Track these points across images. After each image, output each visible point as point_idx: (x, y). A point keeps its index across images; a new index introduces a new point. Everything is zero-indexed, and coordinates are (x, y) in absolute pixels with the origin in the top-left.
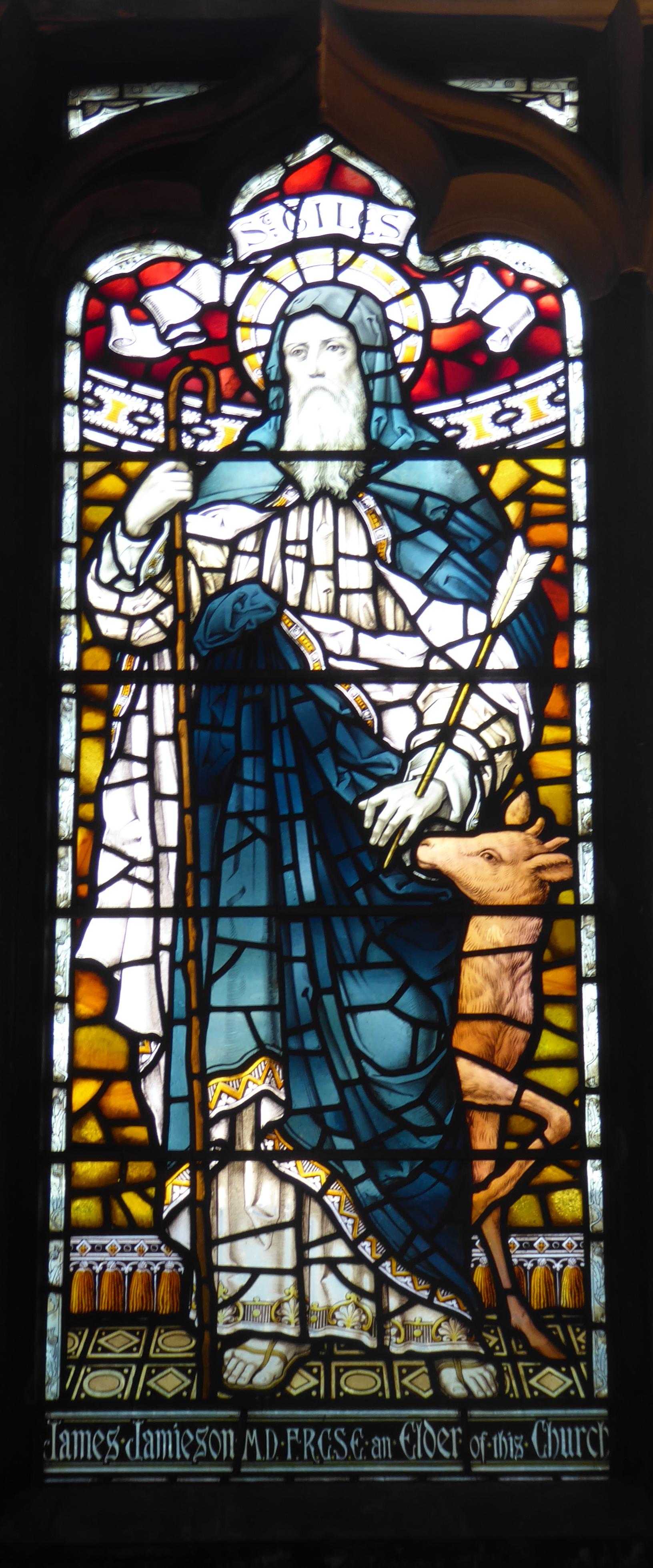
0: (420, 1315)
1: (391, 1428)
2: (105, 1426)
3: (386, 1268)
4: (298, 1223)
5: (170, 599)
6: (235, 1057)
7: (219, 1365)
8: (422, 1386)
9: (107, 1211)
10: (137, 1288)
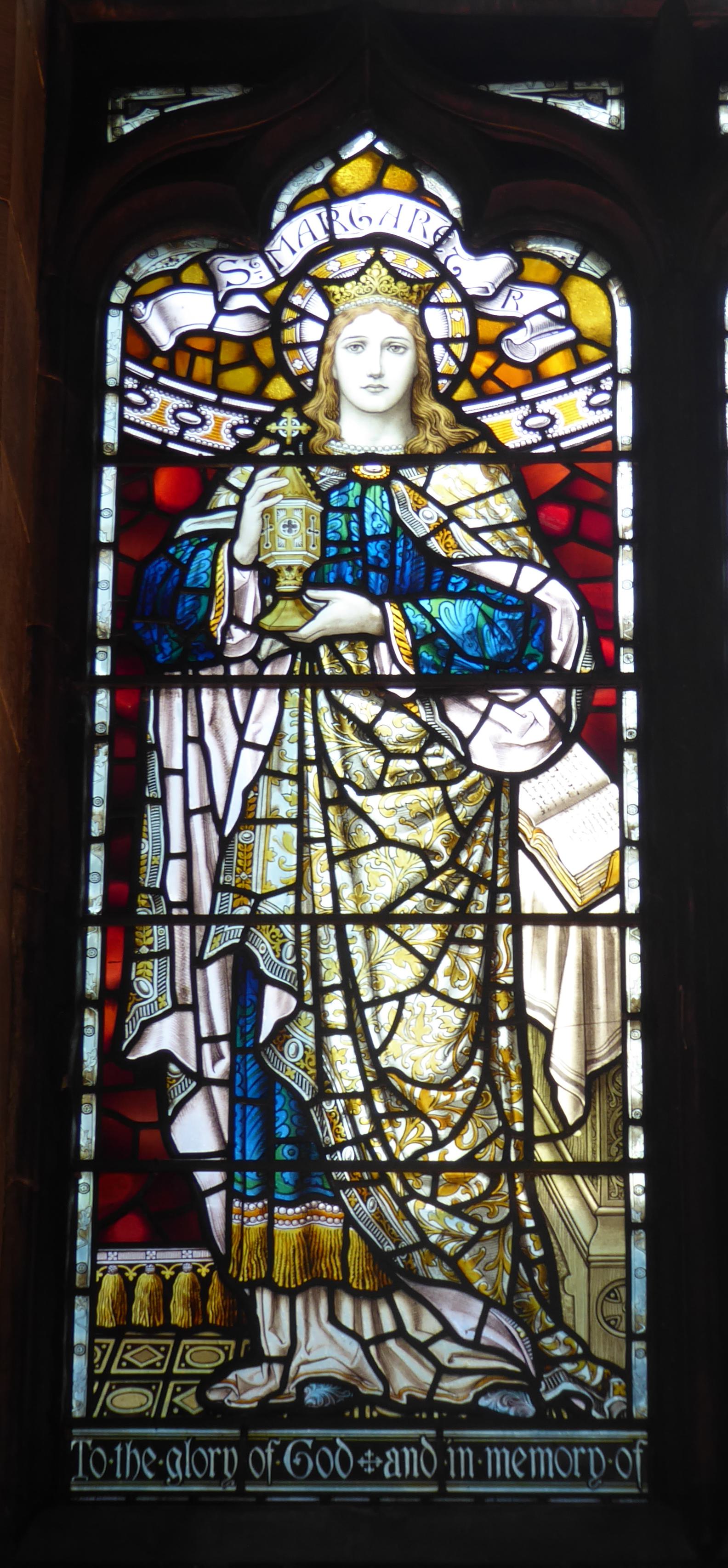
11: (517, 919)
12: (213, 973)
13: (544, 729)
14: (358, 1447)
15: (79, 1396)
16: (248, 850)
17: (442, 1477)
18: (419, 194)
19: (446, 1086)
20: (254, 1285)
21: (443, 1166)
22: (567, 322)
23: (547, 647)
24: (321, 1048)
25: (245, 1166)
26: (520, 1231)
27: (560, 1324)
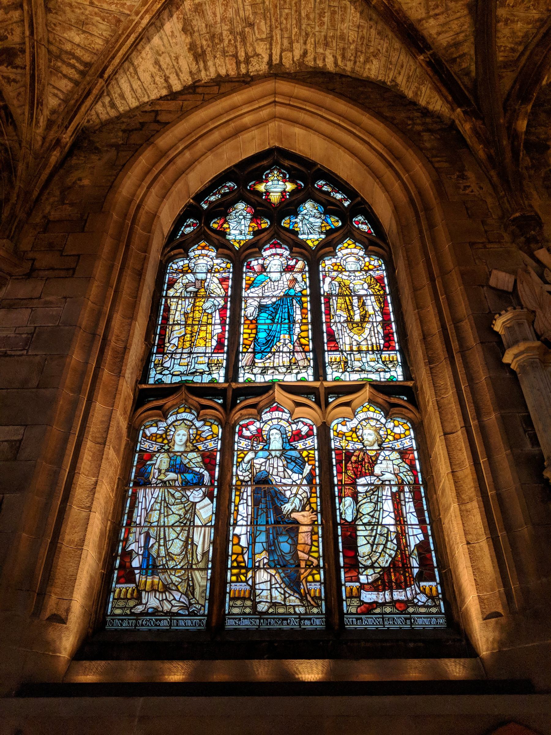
0: (292, 598)
1: (286, 619)
2: (236, 619)
3: (286, 589)
4: (270, 581)
5: (251, 473)
6: (260, 551)
7: (256, 607)
8: (292, 611)
9: (237, 579)
10: (242, 593)
11: (194, 526)
12: (142, 536)
13: (201, 495)
14: (156, 620)
15: (109, 611)
16: (151, 515)
17: (170, 626)
18: (191, 413)
19: (179, 555)
20: (142, 590)
21: (177, 569)
22: (212, 431)
23: (203, 481)
24: (159, 549)
25: (143, 569)
26: (189, 580)
27: (194, 597)
